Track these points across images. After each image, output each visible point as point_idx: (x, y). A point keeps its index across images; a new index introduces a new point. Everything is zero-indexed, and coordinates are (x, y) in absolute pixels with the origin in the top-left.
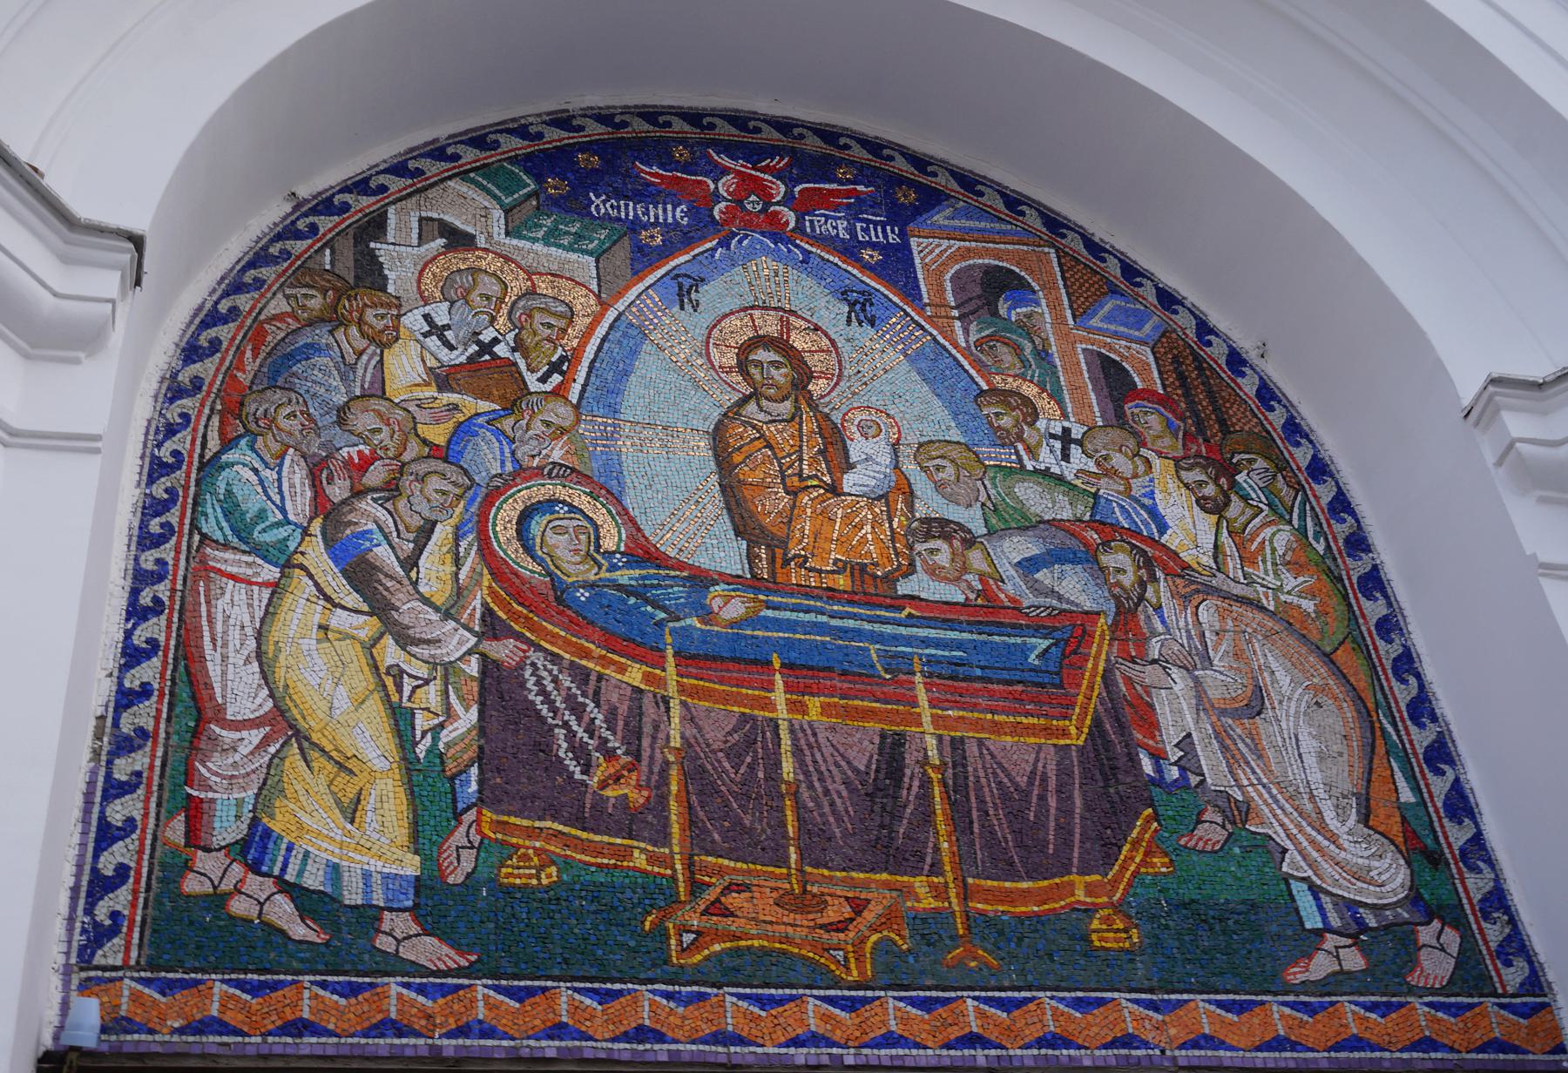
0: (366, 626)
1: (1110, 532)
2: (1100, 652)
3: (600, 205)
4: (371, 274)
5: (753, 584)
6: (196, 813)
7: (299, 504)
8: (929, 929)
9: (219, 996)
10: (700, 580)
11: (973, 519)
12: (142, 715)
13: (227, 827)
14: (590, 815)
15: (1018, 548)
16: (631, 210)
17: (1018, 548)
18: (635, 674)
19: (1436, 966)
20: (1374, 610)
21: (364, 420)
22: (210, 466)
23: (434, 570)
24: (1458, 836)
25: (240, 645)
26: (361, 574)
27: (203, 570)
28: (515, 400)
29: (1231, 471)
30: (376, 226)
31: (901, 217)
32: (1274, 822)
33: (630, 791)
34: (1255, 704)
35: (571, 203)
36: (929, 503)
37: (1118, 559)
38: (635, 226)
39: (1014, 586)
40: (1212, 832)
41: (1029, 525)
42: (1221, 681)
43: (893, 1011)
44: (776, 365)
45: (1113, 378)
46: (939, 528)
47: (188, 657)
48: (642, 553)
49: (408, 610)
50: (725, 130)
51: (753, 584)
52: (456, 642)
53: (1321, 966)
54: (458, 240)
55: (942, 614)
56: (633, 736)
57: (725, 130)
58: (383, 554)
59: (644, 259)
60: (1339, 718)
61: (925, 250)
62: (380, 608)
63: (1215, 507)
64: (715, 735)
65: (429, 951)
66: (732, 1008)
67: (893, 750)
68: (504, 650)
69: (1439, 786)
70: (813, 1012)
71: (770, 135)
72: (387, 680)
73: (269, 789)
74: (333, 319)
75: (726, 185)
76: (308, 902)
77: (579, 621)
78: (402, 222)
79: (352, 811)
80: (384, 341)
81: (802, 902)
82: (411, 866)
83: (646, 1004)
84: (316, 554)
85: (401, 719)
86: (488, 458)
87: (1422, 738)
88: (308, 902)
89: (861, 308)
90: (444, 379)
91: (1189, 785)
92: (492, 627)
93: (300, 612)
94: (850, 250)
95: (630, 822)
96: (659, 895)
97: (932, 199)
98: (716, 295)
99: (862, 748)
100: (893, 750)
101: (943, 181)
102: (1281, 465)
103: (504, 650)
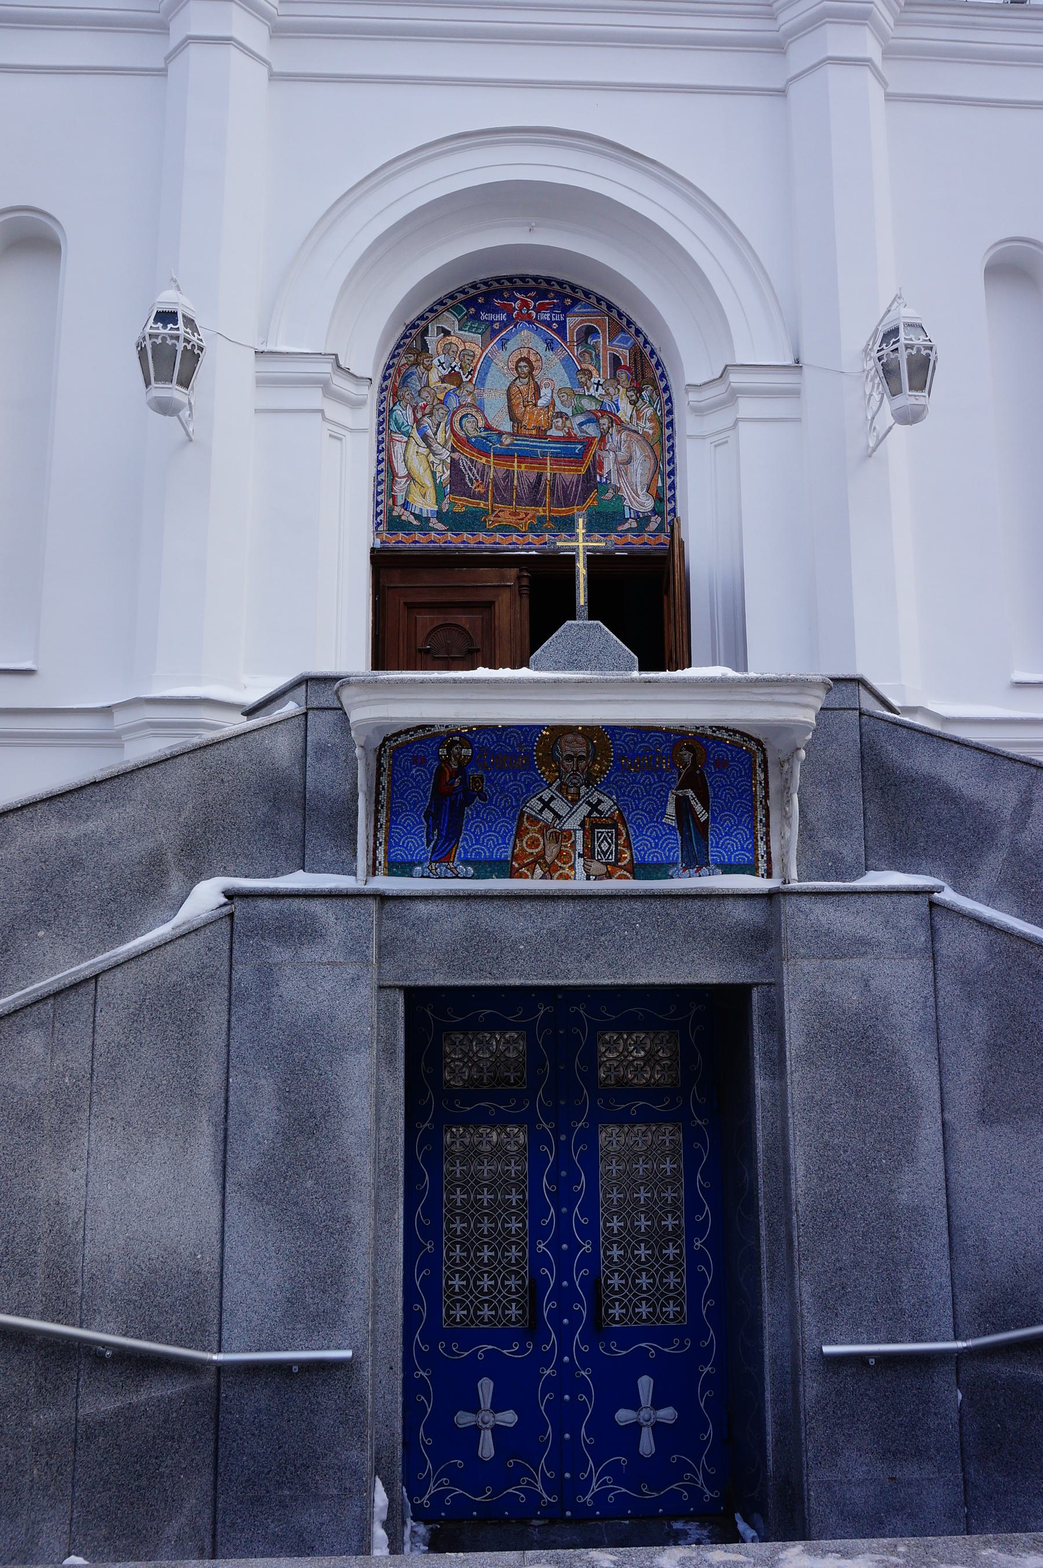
0: (425, 451)
1: (603, 412)
2: (594, 448)
3: (484, 316)
4: (425, 347)
5: (512, 434)
6: (394, 498)
7: (411, 420)
8: (541, 520)
10: (500, 434)
12: (382, 476)
13: (400, 501)
14: (473, 496)
15: (580, 419)
16: (491, 317)
17: (580, 419)
18: (484, 460)
19: (653, 526)
20: (668, 432)
21: (424, 394)
22: (391, 411)
23: (440, 436)
24: (669, 494)
25: (400, 458)
26: (425, 438)
27: (391, 439)
28: (460, 384)
29: (640, 391)
30: (425, 332)
31: (566, 310)
32: (626, 492)
33: (481, 489)
34: (629, 461)
35: (475, 317)
36: (559, 407)
37: (605, 421)
38: (493, 322)
39: (576, 431)
40: (610, 495)
41: (583, 412)
42: (622, 455)
43: (531, 537)
44: (525, 366)
45: (616, 361)
46: (560, 415)
47: (390, 462)
48: (488, 428)
49: (435, 446)
50: (519, 283)
51: (512, 434)
52: (446, 454)
53: (626, 526)
54: (447, 333)
55: (557, 440)
56: (482, 476)
57: (519, 283)
58: (430, 432)
59: (495, 333)
60: (650, 464)
61: (571, 322)
62: (429, 446)
63: (633, 403)
64: (500, 475)
65: (440, 526)
66: (498, 536)
67: (539, 477)
68: (456, 456)
69: (669, 481)
70: (514, 537)
71: (532, 283)
73: (408, 492)
74: (416, 364)
75: (517, 305)
76: (417, 517)
77: (473, 447)
78: (432, 329)
79: (424, 496)
80: (428, 369)
81: (515, 514)
82: (436, 508)
83: (481, 536)
84: (415, 434)
85: (433, 473)
86: (453, 403)
87: (668, 469)
88: (417, 517)
89: (550, 345)
90: (443, 380)
91: (606, 485)
92: (453, 450)
93: (412, 448)
94: (548, 324)
95: (482, 497)
96: (485, 513)
97: (576, 301)
98: (511, 345)
99: (533, 477)
100: (539, 477)
101: (580, 295)
102: (656, 388)
103: (456, 456)
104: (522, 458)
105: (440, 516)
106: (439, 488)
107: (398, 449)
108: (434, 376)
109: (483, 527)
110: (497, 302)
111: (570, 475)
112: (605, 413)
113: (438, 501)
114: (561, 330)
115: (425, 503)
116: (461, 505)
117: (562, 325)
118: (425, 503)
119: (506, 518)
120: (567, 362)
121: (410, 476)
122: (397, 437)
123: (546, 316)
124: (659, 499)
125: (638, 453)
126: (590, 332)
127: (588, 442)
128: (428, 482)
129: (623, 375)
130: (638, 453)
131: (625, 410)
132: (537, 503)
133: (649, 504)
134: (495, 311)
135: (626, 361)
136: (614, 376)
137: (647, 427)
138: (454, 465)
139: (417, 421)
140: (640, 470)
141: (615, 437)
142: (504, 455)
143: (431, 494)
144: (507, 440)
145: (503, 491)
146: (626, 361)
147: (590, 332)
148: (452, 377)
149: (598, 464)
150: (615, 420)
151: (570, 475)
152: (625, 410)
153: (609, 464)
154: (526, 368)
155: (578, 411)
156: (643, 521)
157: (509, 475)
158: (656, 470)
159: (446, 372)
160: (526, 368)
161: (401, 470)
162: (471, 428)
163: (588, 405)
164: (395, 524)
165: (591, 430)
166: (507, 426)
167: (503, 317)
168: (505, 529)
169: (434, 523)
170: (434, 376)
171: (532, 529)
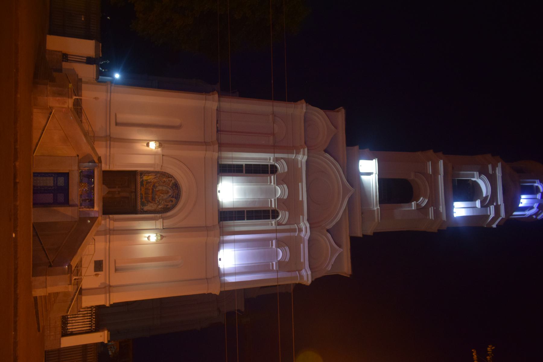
0: (153, 178)
1: (160, 203)
2: (154, 202)
4: (169, 178)
5: (156, 190)
7: (158, 176)
8: (142, 195)
10: (156, 189)
11: (160, 198)
14: (146, 184)
15: (158, 200)
17: (158, 200)
23: (155, 180)
26: (155, 178)
28: (163, 183)
30: (171, 178)
31: (175, 198)
33: (147, 186)
34: (152, 207)
36: (160, 197)
40: (146, 204)
43: (140, 193)
45: (167, 205)
46: (159, 197)
47: (150, 173)
48: (157, 187)
49: (153, 179)
51: (156, 190)
52: (152, 181)
53: (142, 207)
57: (179, 191)
58: (156, 179)
59: (171, 188)
62: (153, 178)
63: (161, 208)
65: (141, 180)
71: (179, 193)
73: (146, 176)
74: (166, 177)
75: (176, 191)
76: (142, 177)
78: (172, 179)
79: (146, 178)
80: (166, 178)
82: (144, 179)
84: (156, 176)
85: (149, 179)
86: (160, 182)
88: (142, 177)
89: (170, 196)
90: (164, 181)
92: (153, 182)
94: (173, 195)
95: (146, 186)
96: (143, 186)
97: (177, 199)
100: (149, 194)
101: (178, 200)
104: (152, 192)
105: (143, 180)
106: (147, 180)
107: (153, 174)
108: (165, 179)
109: (141, 186)
110: (176, 188)
111: (150, 199)
113: (145, 180)
114: (173, 197)
115: (145, 178)
116: (145, 183)
117: (173, 197)
119: (143, 189)
121: (149, 176)
122: (155, 174)
123: (174, 195)
126: (172, 201)
127: (155, 201)
128: (148, 178)
129: (165, 206)
131: (160, 207)
132: (145, 194)
134: (175, 188)
135: (168, 207)
138: (151, 182)
139: (157, 177)
143: (146, 179)
144: (155, 190)
146: (168, 207)
147: (172, 201)
148: (164, 182)
149: (151, 202)
150: (158, 205)
152: (160, 207)
157: (149, 190)
159: (165, 181)
161: (150, 175)
162: (157, 184)
165: (157, 202)
166: (157, 189)
167: (174, 189)
168: (141, 189)
169: (141, 179)
170: (165, 179)
171: (141, 193)
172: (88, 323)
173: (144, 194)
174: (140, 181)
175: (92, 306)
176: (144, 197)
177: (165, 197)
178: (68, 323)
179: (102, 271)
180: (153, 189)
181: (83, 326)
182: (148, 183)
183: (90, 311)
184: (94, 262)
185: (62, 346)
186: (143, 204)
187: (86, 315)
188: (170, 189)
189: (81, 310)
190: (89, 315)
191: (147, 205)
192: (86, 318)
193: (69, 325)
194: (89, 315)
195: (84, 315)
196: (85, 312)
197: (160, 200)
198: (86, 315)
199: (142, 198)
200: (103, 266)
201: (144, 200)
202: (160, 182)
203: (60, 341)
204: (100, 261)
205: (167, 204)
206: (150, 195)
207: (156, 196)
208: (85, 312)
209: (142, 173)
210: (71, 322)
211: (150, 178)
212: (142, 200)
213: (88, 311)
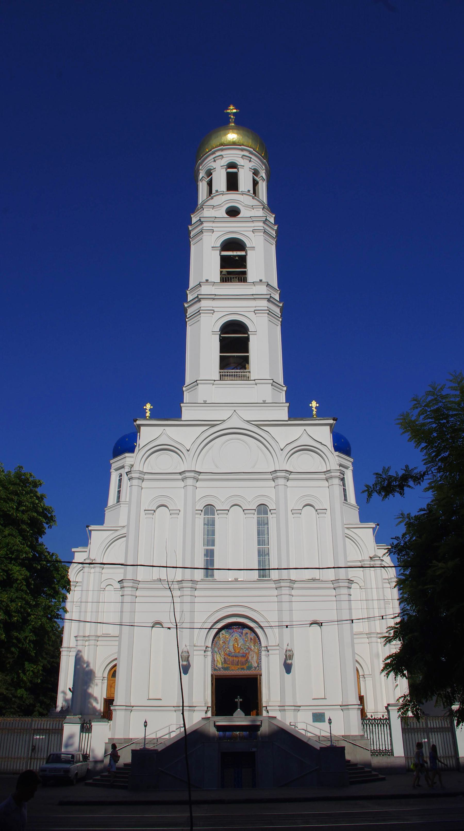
0: (219, 656)
2: (247, 655)
3: (229, 631)
6: (215, 665)
7: (217, 651)
8: (239, 668)
9: (216, 671)
10: (232, 653)
11: (243, 648)
12: (213, 661)
13: (216, 665)
14: (228, 664)
16: (231, 631)
17: (245, 649)
18: (229, 657)
19: (257, 669)
20: (260, 652)
21: (219, 645)
22: (214, 649)
23: (222, 653)
24: (260, 663)
26: (220, 653)
27: (214, 654)
29: (255, 644)
32: (253, 663)
33: (229, 663)
34: (253, 657)
35: (228, 631)
36: (242, 647)
37: (249, 650)
38: (231, 632)
39: (244, 652)
40: (250, 663)
42: (252, 656)
45: (251, 638)
48: (230, 651)
49: (221, 655)
52: (223, 656)
53: (253, 669)
54: (223, 634)
56: (229, 660)
58: (220, 652)
59: (231, 634)
60: (257, 657)
62: (220, 655)
63: (254, 646)
64: (232, 660)
65: (222, 670)
66: (232, 671)
67: (238, 660)
68: (225, 657)
69: (260, 661)
70: (234, 671)
72: (221, 658)
76: (219, 668)
77: (227, 655)
79: (220, 664)
80: (220, 641)
81: (235, 667)
84: (218, 653)
85: (221, 660)
86: (224, 647)
87: (260, 658)
88: (219, 668)
89: (240, 636)
90: (222, 643)
91: (250, 661)
92: (224, 656)
93: (218, 655)
95: (229, 664)
96: (230, 667)
98: (234, 636)
99: (238, 660)
100: (238, 660)
102: (258, 643)
103: (225, 657)
104: (236, 657)
105: (222, 668)
106: (222, 663)
107: (215, 656)
108: (221, 642)
109: (229, 670)
111: (244, 660)
112: (249, 648)
113: (222, 665)
114: (242, 633)
115: (220, 666)
116: (226, 666)
117: (242, 632)
118: (220, 666)
120: (243, 639)
121: (217, 660)
122: (215, 653)
124: (258, 664)
125: (255, 655)
126: (247, 633)
127: (246, 654)
128: (220, 662)
129: (252, 641)
130: (255, 655)
132: (238, 665)
133: (256, 665)
135: (253, 639)
136: (251, 641)
137: (256, 650)
138: (224, 658)
140: (255, 658)
141: (251, 653)
142: (233, 656)
143: (221, 664)
144: (233, 654)
145: (232, 663)
147: (247, 633)
148: (224, 642)
149: (248, 658)
150: (251, 649)
151: (244, 660)
152: (253, 647)
153: (250, 658)
154: (236, 640)
155: (245, 648)
156: (256, 668)
157: (233, 660)
158: (258, 659)
159: (223, 641)
160: (236, 640)
161: (216, 660)
162: (227, 652)
163: (246, 647)
164: (215, 669)
165: (247, 651)
169: (221, 669)
170: (221, 642)
172: (379, 727)
173: (239, 667)
174: (224, 671)
175: (362, 723)
176: (242, 667)
177: (241, 642)
178: (380, 750)
179: (324, 713)
180: (233, 656)
181: (383, 733)
182: (225, 662)
183: (367, 726)
184: (314, 723)
185: (403, 755)
186: (250, 668)
187: (371, 730)
188: (232, 636)
189: (366, 736)
190: (371, 727)
191: (251, 662)
192: (374, 730)
193: (381, 749)
194: (371, 727)
195: (371, 732)
196: (368, 731)
197: (245, 648)
198: (371, 730)
199: (243, 669)
200: (318, 713)
201: (245, 667)
202: (224, 647)
203: (397, 757)
204: (313, 716)
205: (249, 639)
206: (240, 660)
207: (241, 652)
208: (368, 731)
209: (214, 668)
210: (378, 746)
211: (219, 658)
212: (245, 668)
213: (367, 728)
